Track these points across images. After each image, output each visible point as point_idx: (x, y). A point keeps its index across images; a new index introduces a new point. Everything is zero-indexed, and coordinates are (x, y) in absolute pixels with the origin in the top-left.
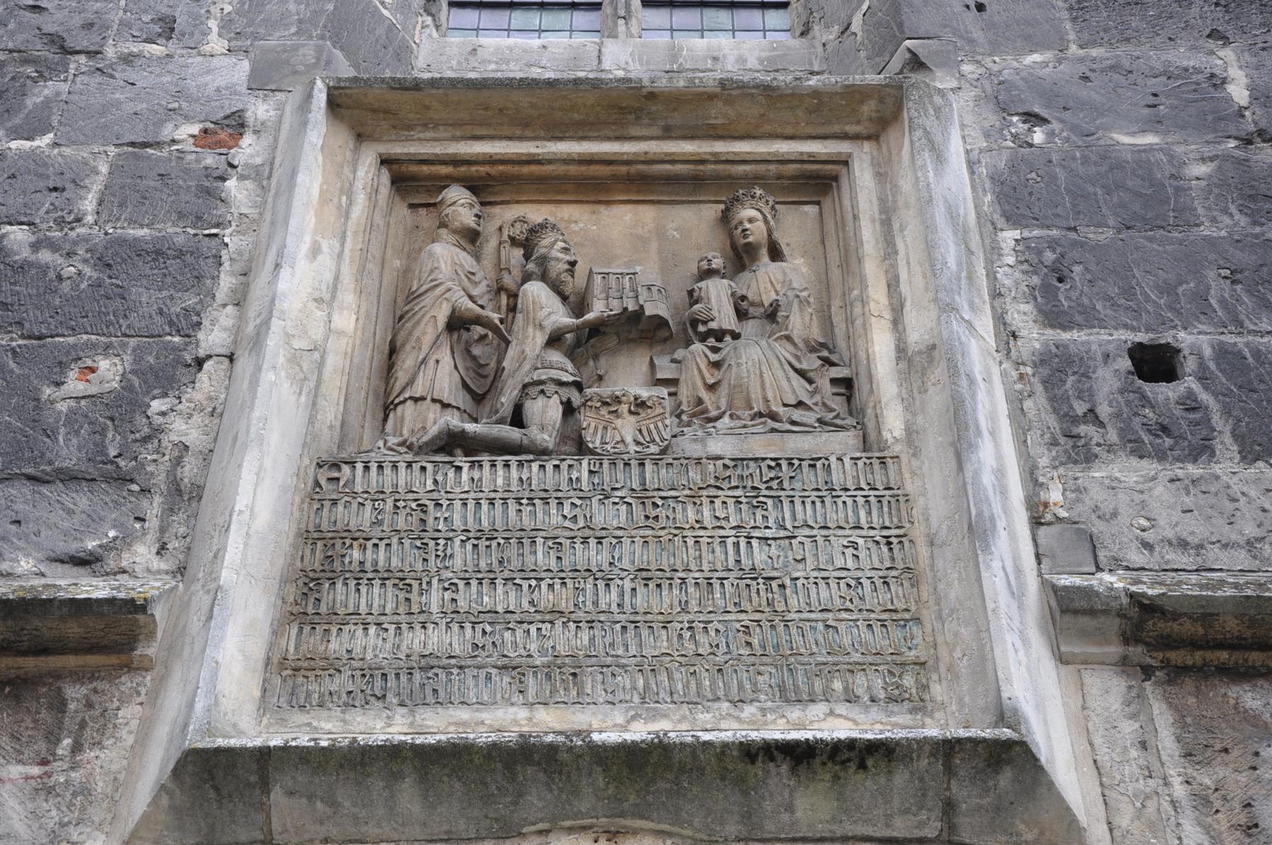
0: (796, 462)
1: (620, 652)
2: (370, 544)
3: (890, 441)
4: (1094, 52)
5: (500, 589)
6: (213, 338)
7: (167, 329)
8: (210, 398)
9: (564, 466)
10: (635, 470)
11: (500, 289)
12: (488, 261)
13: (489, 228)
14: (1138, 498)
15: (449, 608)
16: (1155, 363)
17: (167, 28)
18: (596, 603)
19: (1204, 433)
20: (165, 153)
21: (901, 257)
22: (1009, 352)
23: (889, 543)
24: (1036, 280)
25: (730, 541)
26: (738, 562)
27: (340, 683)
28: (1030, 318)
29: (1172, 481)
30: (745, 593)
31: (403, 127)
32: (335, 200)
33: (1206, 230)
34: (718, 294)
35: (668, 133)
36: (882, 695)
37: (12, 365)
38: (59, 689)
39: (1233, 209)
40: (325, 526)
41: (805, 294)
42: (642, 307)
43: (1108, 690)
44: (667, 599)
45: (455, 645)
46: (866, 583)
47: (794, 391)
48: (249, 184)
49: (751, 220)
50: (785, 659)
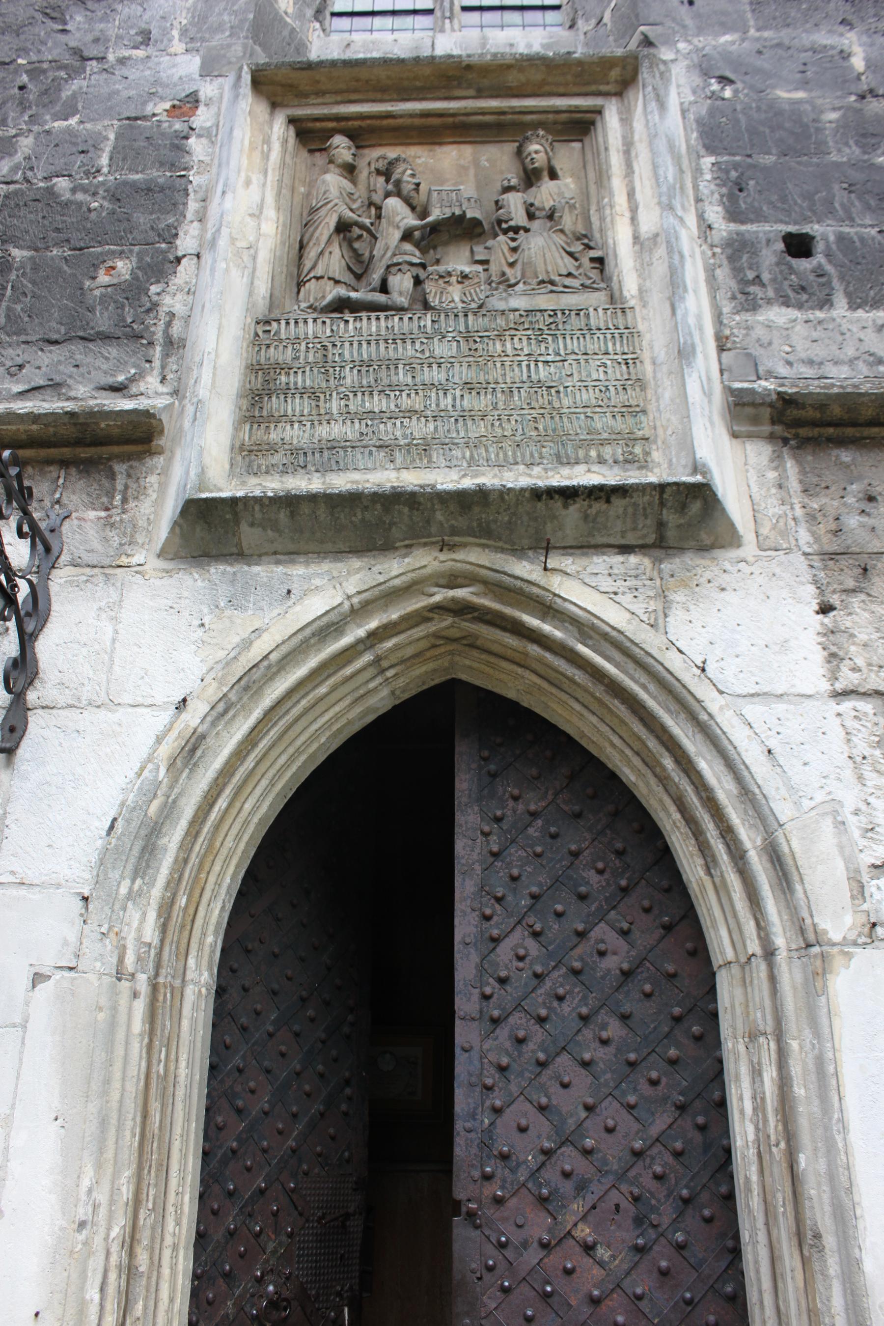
0: (567, 312)
1: (454, 435)
2: (292, 372)
3: (628, 297)
5: (376, 398)
6: (186, 243)
7: (157, 239)
8: (186, 283)
9: (415, 318)
10: (462, 319)
11: (371, 204)
12: (362, 185)
13: (362, 164)
14: (785, 333)
15: (345, 410)
16: (799, 246)
17: (146, 38)
18: (438, 405)
19: (827, 291)
21: (636, 175)
22: (706, 238)
23: (627, 364)
24: (724, 190)
25: (524, 364)
26: (529, 377)
27: (278, 458)
28: (722, 215)
29: (806, 322)
30: (534, 397)
31: (302, 96)
32: (260, 148)
33: (834, 157)
34: (515, 204)
35: (480, 94)
36: (621, 458)
37: (66, 268)
38: (111, 467)
39: (851, 142)
40: (263, 361)
41: (572, 201)
42: (464, 212)
43: (758, 453)
44: (483, 402)
45: (349, 433)
46: (612, 389)
47: (566, 266)
48: (204, 141)
49: (536, 152)
50: (559, 437)
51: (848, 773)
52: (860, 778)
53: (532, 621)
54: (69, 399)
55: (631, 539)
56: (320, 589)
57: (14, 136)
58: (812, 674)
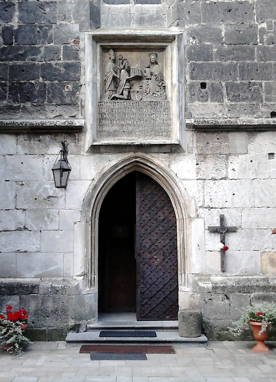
4: (205, 24)
16: (203, 85)
20: (69, 45)
33: (214, 62)
51: (197, 192)
52: (199, 193)
53: (149, 165)
54: (64, 119)
55: (166, 151)
56: (114, 160)
57: (40, 47)
58: (194, 176)
